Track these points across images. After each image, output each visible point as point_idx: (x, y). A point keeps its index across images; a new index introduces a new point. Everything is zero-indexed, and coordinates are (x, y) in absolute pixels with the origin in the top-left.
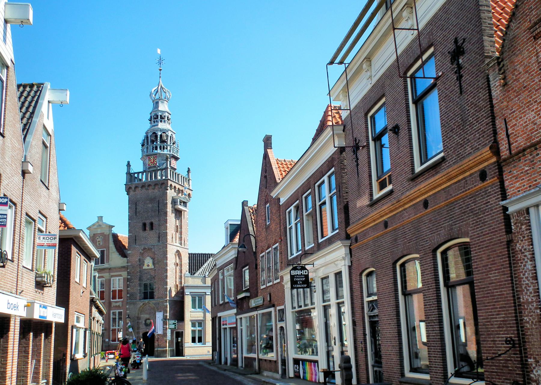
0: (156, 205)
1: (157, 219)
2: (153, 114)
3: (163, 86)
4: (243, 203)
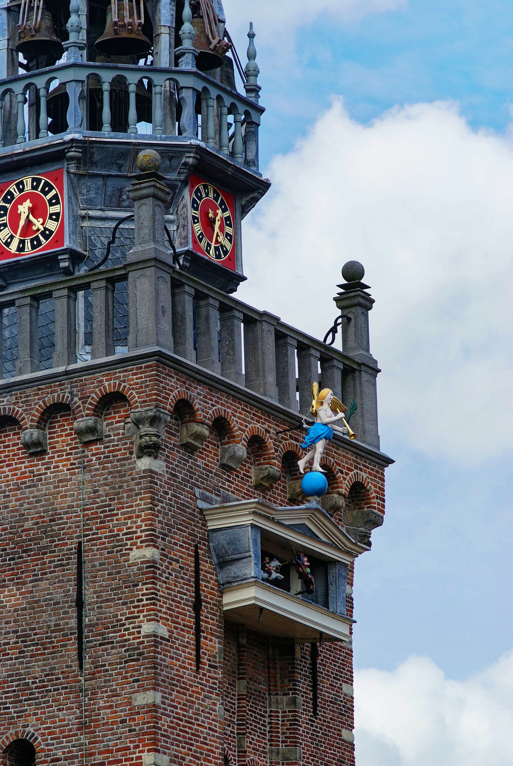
0: (57, 588)
1: (70, 718)
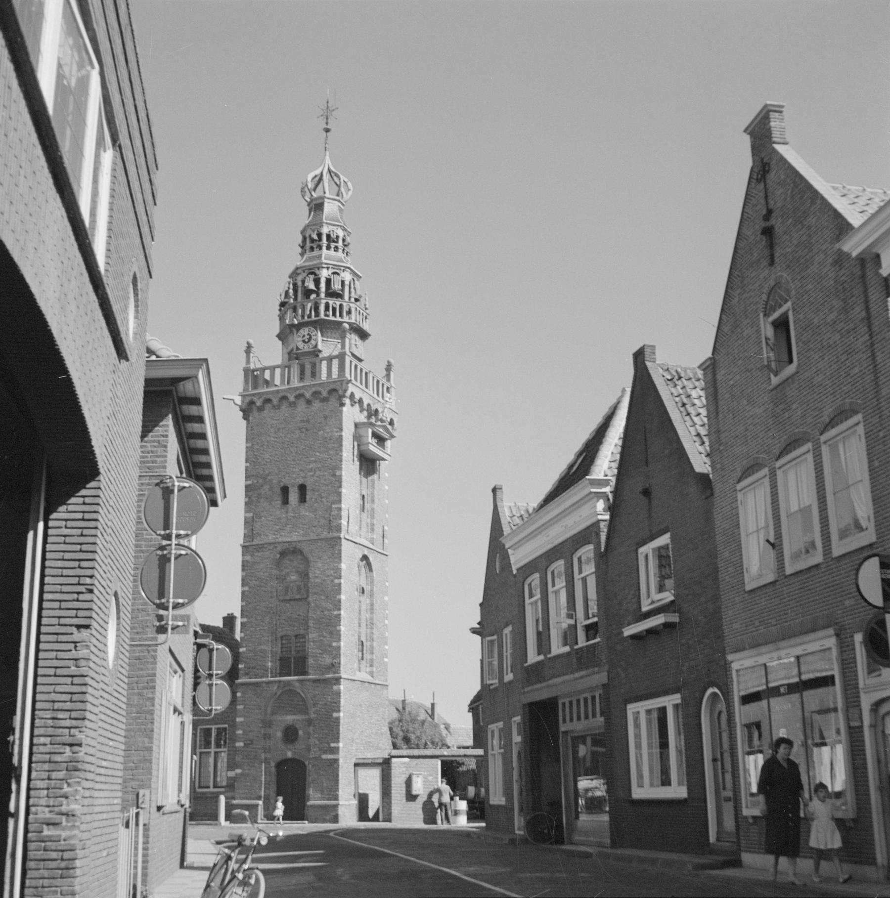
3: (333, 169)
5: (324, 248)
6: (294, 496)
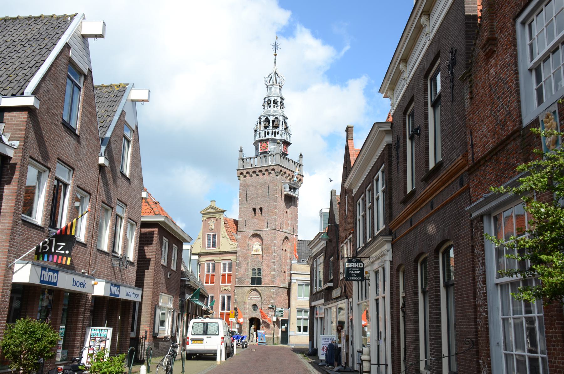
1: (266, 205)
2: (267, 100)
4: (331, 192)
5: (272, 107)
6: (258, 211)
